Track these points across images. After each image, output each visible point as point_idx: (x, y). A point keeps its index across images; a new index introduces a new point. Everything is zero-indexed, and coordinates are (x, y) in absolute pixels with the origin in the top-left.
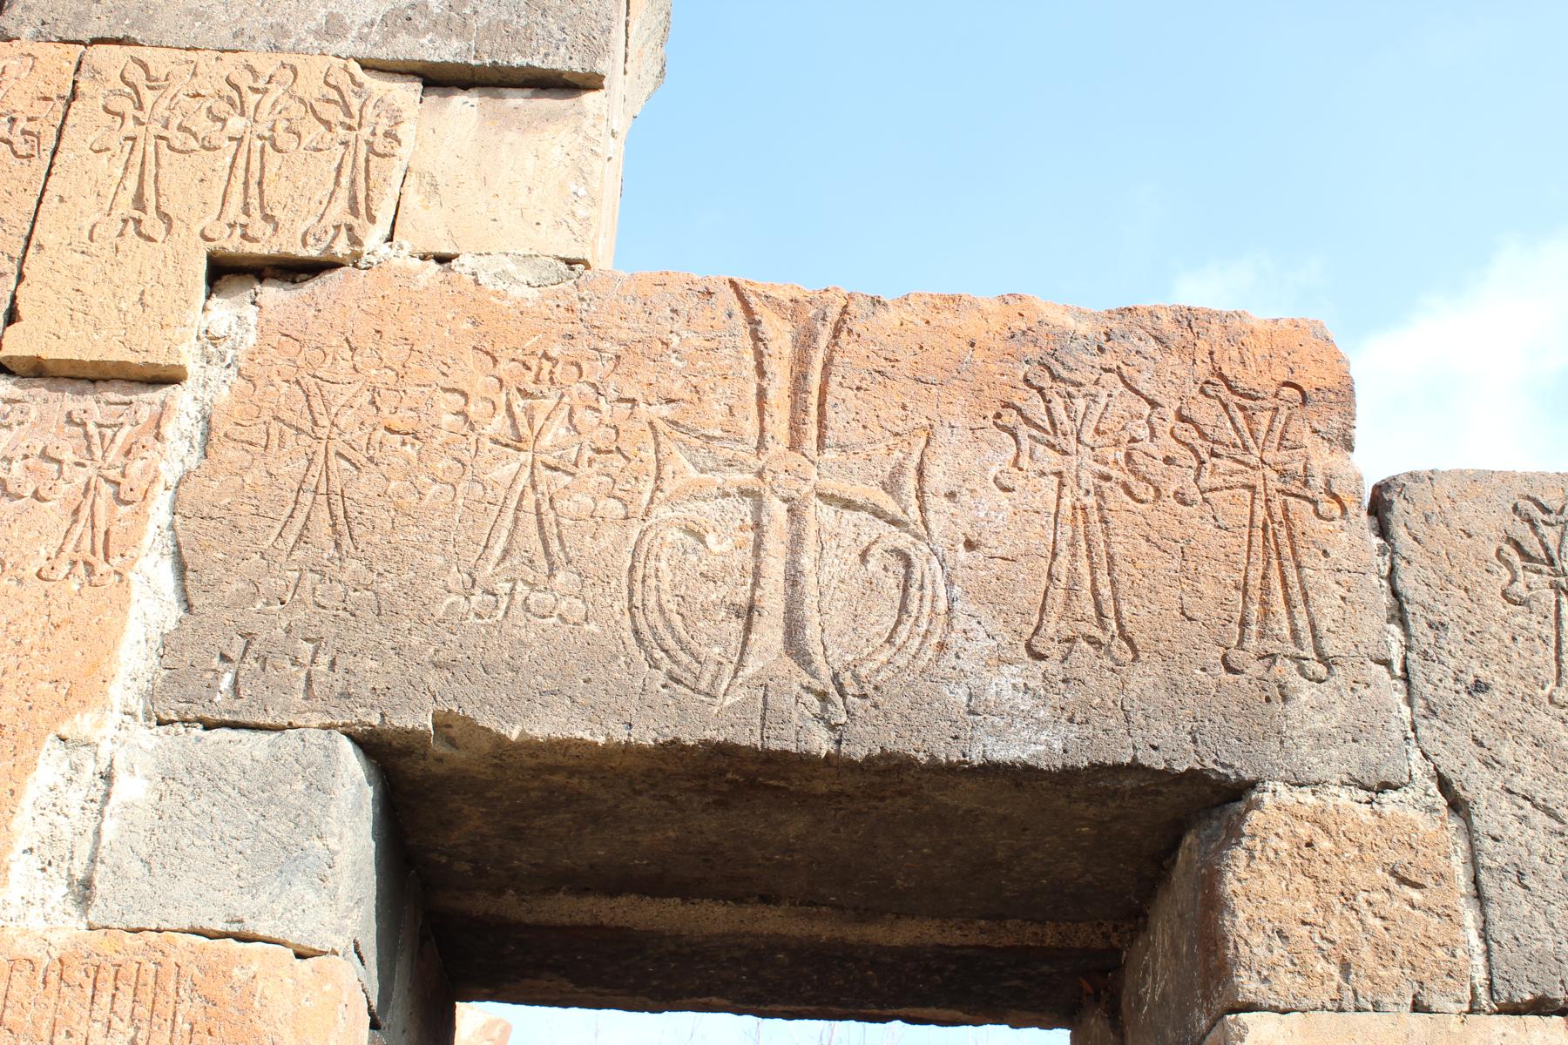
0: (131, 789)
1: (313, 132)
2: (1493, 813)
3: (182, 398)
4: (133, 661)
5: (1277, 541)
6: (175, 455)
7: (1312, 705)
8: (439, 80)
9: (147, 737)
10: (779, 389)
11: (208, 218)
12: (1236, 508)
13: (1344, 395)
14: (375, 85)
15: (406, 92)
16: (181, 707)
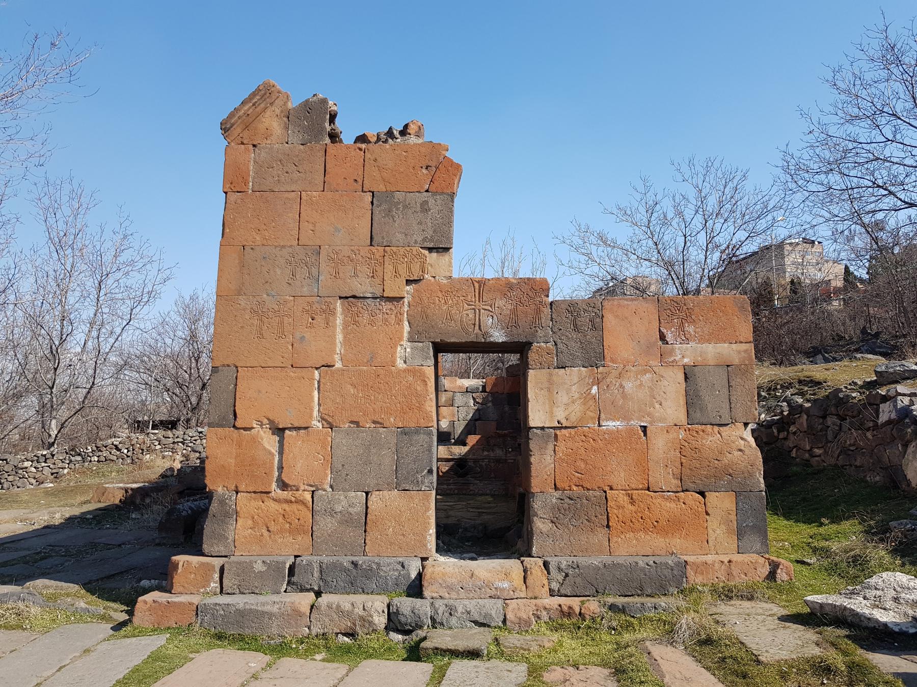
0: (408, 350)
1: (416, 260)
2: (560, 345)
3: (406, 300)
4: (406, 335)
5: (538, 311)
6: (406, 308)
7: (540, 333)
8: (430, 250)
9: (409, 344)
10: (477, 291)
11: (405, 275)
12: (533, 306)
13: (548, 289)
14: (423, 251)
15: (426, 252)
16: (411, 340)
